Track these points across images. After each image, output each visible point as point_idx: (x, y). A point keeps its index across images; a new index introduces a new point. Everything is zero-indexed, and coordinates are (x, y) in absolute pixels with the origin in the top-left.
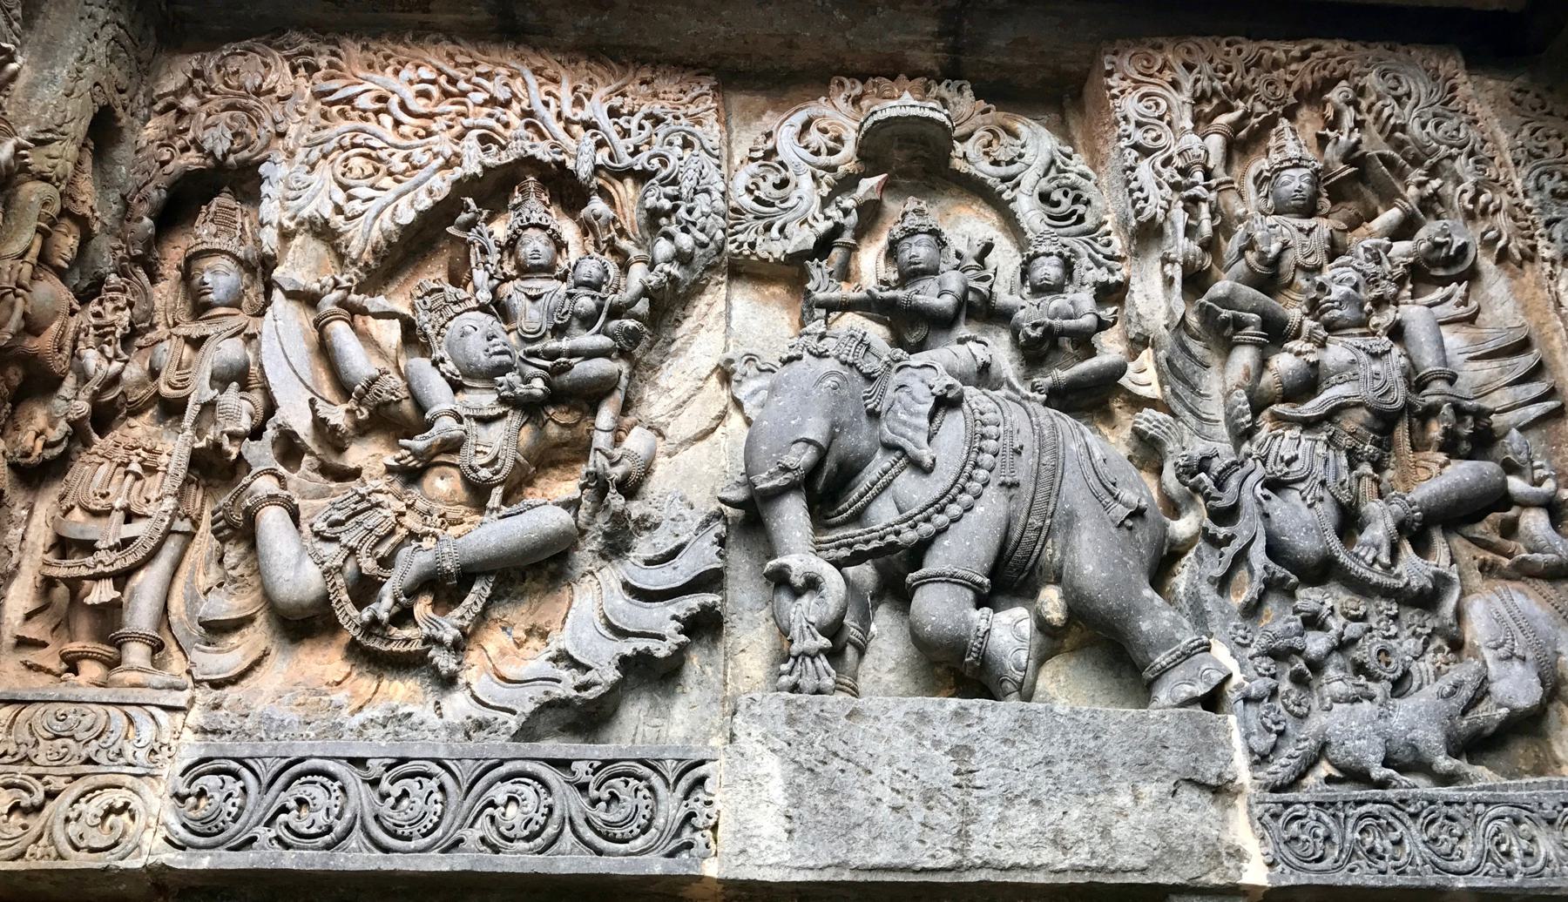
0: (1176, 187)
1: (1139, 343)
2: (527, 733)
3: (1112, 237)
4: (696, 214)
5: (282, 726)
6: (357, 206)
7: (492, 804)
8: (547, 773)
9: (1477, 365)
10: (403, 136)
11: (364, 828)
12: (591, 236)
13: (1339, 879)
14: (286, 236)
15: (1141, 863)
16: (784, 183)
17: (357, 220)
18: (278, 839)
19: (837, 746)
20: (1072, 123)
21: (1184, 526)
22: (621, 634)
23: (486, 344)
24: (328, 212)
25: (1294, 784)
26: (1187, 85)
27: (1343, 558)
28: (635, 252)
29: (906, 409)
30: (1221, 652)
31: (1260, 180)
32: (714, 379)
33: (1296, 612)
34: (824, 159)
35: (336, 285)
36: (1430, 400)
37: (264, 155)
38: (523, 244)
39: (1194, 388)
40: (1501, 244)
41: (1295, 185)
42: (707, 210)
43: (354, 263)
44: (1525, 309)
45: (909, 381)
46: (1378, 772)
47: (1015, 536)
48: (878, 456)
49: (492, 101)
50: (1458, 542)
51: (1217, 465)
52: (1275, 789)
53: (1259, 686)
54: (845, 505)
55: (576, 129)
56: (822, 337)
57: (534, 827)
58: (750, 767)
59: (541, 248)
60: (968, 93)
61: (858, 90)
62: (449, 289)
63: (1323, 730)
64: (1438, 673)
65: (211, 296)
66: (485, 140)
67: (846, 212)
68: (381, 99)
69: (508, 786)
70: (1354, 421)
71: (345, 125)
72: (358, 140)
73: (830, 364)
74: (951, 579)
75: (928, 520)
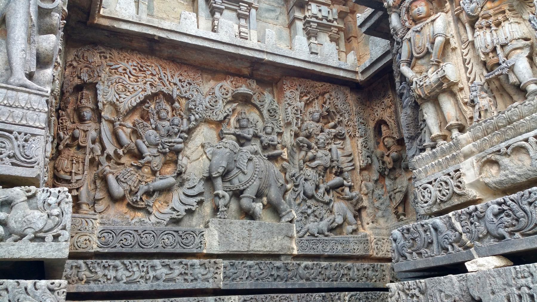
0: (295, 114)
1: (284, 147)
2: (167, 225)
3: (281, 122)
4: (199, 110)
5: (117, 223)
6: (122, 100)
7: (163, 239)
8: (174, 233)
9: (342, 157)
10: (131, 81)
11: (138, 244)
12: (175, 111)
13: (308, 253)
14: (104, 105)
15: (278, 250)
16: (216, 101)
17: (122, 104)
18: (121, 246)
19: (228, 229)
20: (274, 90)
21: (289, 186)
22: (185, 205)
23: (155, 138)
24: (115, 100)
25: (303, 237)
26: (299, 90)
27: (316, 195)
28: (185, 116)
29: (242, 161)
30: (294, 212)
31: (310, 113)
32: (200, 147)
33: (307, 205)
34: (225, 96)
35: (119, 120)
36: (334, 165)
37: (96, 81)
38: (161, 113)
39: (293, 158)
40: (350, 133)
41: (317, 116)
42: (202, 109)
43: (121, 114)
44: (352, 147)
45: (243, 154)
46: (316, 235)
47: (260, 188)
48: (235, 169)
49: (152, 74)
50: (334, 192)
51: (297, 175)
52: (300, 237)
53: (299, 218)
54: (227, 178)
55: (172, 84)
56: (226, 143)
57: (172, 243)
58: (212, 233)
59: (165, 114)
60: (255, 83)
61: (232, 79)
62: (144, 122)
63: (308, 227)
64: (328, 217)
65: (86, 118)
66: (151, 85)
67: (230, 112)
68: (124, 70)
69: (166, 236)
70: (320, 168)
71: (116, 76)
72: (120, 81)
73: (228, 150)
74: (249, 197)
75: (245, 185)
